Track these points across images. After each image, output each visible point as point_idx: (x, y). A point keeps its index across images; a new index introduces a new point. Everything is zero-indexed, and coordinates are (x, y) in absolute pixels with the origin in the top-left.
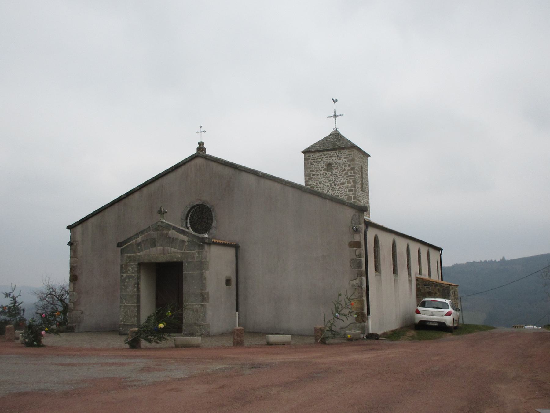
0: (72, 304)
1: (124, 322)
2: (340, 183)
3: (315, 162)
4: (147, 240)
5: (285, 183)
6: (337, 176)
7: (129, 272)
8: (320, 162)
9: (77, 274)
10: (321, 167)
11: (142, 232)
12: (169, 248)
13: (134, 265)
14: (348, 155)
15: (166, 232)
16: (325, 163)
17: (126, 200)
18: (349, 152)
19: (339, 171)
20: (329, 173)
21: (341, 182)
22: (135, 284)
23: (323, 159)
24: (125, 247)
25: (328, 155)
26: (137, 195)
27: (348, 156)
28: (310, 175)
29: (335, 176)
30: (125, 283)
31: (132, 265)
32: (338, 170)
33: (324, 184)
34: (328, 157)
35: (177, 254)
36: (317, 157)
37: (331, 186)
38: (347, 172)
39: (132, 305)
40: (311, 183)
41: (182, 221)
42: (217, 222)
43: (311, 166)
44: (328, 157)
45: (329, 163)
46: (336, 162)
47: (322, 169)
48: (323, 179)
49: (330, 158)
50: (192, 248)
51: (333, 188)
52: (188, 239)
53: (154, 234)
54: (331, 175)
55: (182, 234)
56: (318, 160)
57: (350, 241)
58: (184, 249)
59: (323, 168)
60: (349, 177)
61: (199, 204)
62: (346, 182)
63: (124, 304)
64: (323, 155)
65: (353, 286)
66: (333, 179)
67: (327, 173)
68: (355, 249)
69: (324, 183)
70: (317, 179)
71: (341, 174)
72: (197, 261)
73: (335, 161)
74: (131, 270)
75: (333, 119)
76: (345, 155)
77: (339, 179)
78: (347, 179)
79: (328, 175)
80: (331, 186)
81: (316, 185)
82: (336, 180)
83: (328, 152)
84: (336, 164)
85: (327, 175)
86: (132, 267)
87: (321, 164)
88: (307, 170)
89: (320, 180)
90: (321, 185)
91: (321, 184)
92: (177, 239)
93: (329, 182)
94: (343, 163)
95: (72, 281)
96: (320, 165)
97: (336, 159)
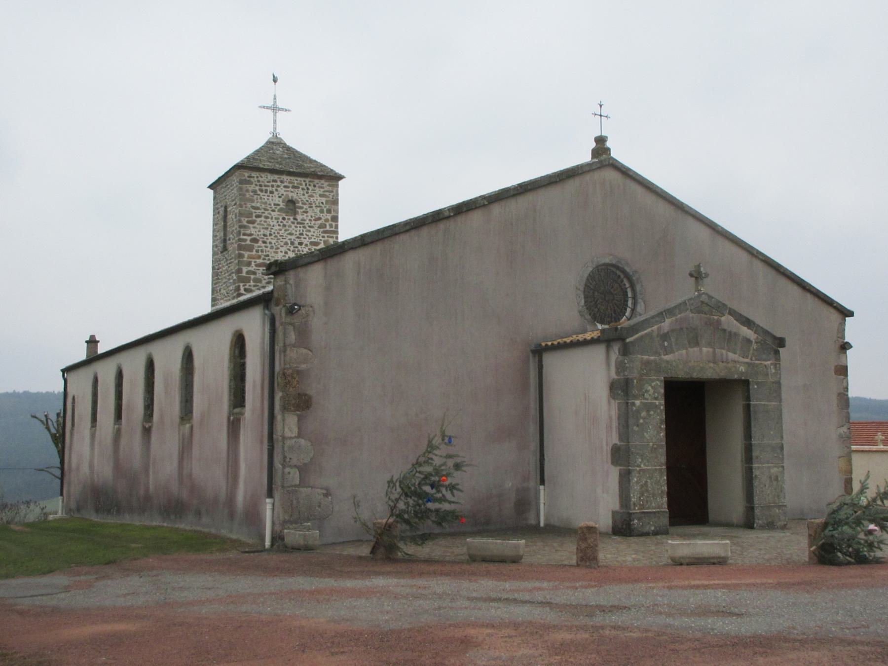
0: (297, 470)
1: (642, 507)
2: (310, 241)
3: (261, 191)
4: (681, 329)
5: (757, 253)
6: (304, 227)
7: (646, 395)
8: (272, 192)
9: (311, 392)
10: (275, 205)
11: (670, 312)
12: (724, 352)
13: (658, 382)
14: (327, 191)
15: (716, 318)
16: (283, 197)
17: (451, 224)
18: (329, 185)
19: (310, 218)
20: (289, 219)
21: (313, 240)
22: (661, 424)
23: (279, 189)
24: (637, 339)
25: (290, 183)
26: (476, 217)
27: (327, 194)
28: (252, 214)
29: (302, 226)
30: (638, 420)
31: (653, 381)
32: (307, 216)
33: (279, 237)
34: (287, 187)
35: (738, 366)
36: (268, 182)
37: (292, 243)
38: (324, 223)
39: (656, 469)
40: (252, 231)
41: (579, 292)
42: (644, 303)
43: (253, 197)
44: (287, 187)
45: (290, 198)
46: (305, 200)
47: (276, 208)
48: (278, 227)
49: (292, 190)
50: (764, 357)
51: (296, 249)
52: (757, 338)
53: (695, 319)
54: (293, 223)
55: (745, 326)
56: (269, 189)
57: (836, 364)
58: (750, 357)
59: (278, 207)
60: (328, 233)
61: (610, 262)
62: (322, 242)
63: (639, 466)
64: (278, 180)
65: (841, 436)
66: (296, 231)
67: (286, 217)
68: (843, 377)
69: (278, 235)
70: (266, 226)
71: (312, 225)
72: (773, 383)
73: (302, 197)
74: (651, 391)
75: (270, 113)
76: (322, 190)
77: (308, 233)
78: (323, 237)
79: (287, 222)
80: (292, 243)
81: (263, 238)
82: (302, 234)
83: (289, 178)
84: (305, 204)
85: (285, 222)
86: (653, 384)
87: (274, 198)
88: (245, 204)
89: (272, 229)
90: (272, 239)
91: (272, 237)
92: (736, 335)
93: (290, 237)
94: (317, 204)
95: (295, 411)
96: (272, 200)
97: (304, 195)
